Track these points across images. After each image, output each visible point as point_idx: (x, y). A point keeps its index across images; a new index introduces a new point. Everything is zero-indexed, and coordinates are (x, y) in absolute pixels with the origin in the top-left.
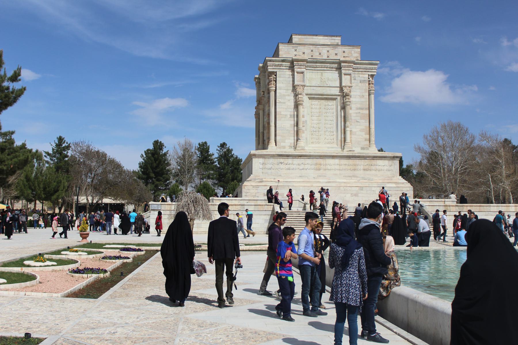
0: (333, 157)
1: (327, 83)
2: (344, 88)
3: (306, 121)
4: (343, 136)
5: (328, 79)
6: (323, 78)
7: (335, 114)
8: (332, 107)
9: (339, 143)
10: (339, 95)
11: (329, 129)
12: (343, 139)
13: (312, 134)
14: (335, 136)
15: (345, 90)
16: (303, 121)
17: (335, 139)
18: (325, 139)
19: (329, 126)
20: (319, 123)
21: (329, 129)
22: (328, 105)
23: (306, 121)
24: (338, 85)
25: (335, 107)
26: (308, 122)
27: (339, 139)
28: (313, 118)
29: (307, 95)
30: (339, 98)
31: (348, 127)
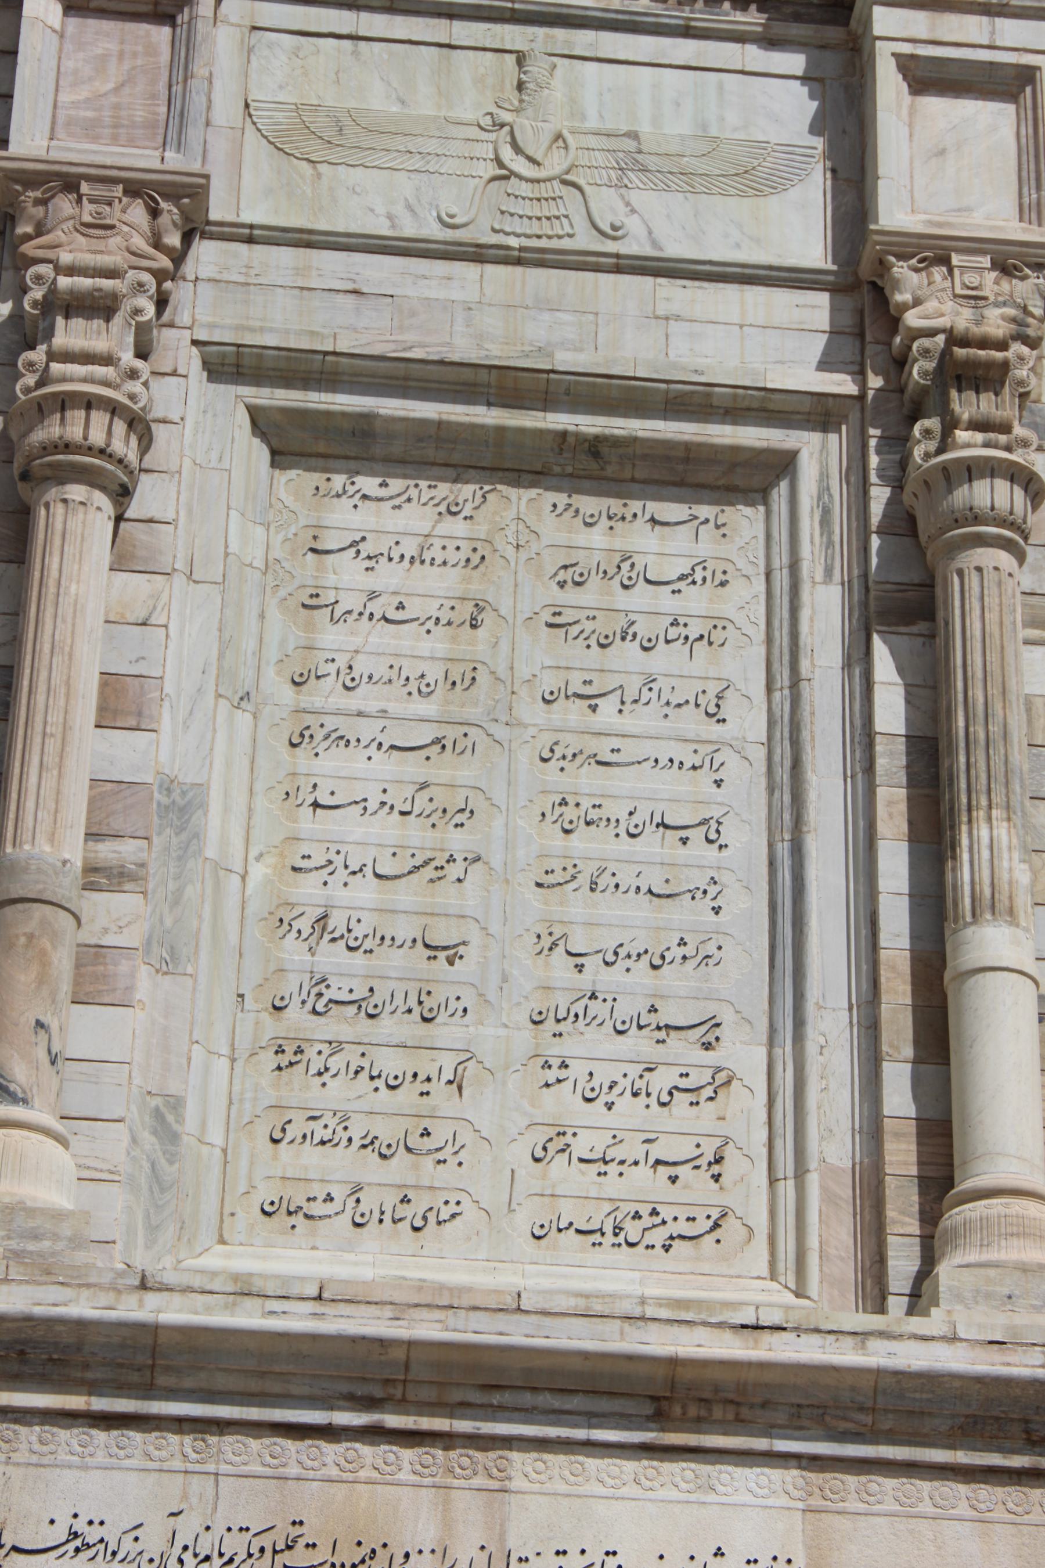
0: (672, 1406)
1: (607, 205)
2: (907, 280)
3: (181, 806)
4: (899, 1097)
5: (633, 159)
6: (534, 134)
7: (748, 720)
8: (695, 601)
9: (833, 1235)
10: (819, 413)
11: (631, 986)
12: (902, 1156)
13: (289, 1056)
14: (747, 1104)
15: (930, 305)
16: (110, 803)
17: (747, 1172)
18: (555, 1143)
19: (630, 920)
20: (431, 867)
21: (631, 986)
22: (624, 570)
23: (181, 806)
24: (812, 250)
25: (744, 602)
26: (220, 827)
27: (834, 1146)
28: (330, 768)
29: (228, 365)
30: (818, 455)
31: (994, 905)
